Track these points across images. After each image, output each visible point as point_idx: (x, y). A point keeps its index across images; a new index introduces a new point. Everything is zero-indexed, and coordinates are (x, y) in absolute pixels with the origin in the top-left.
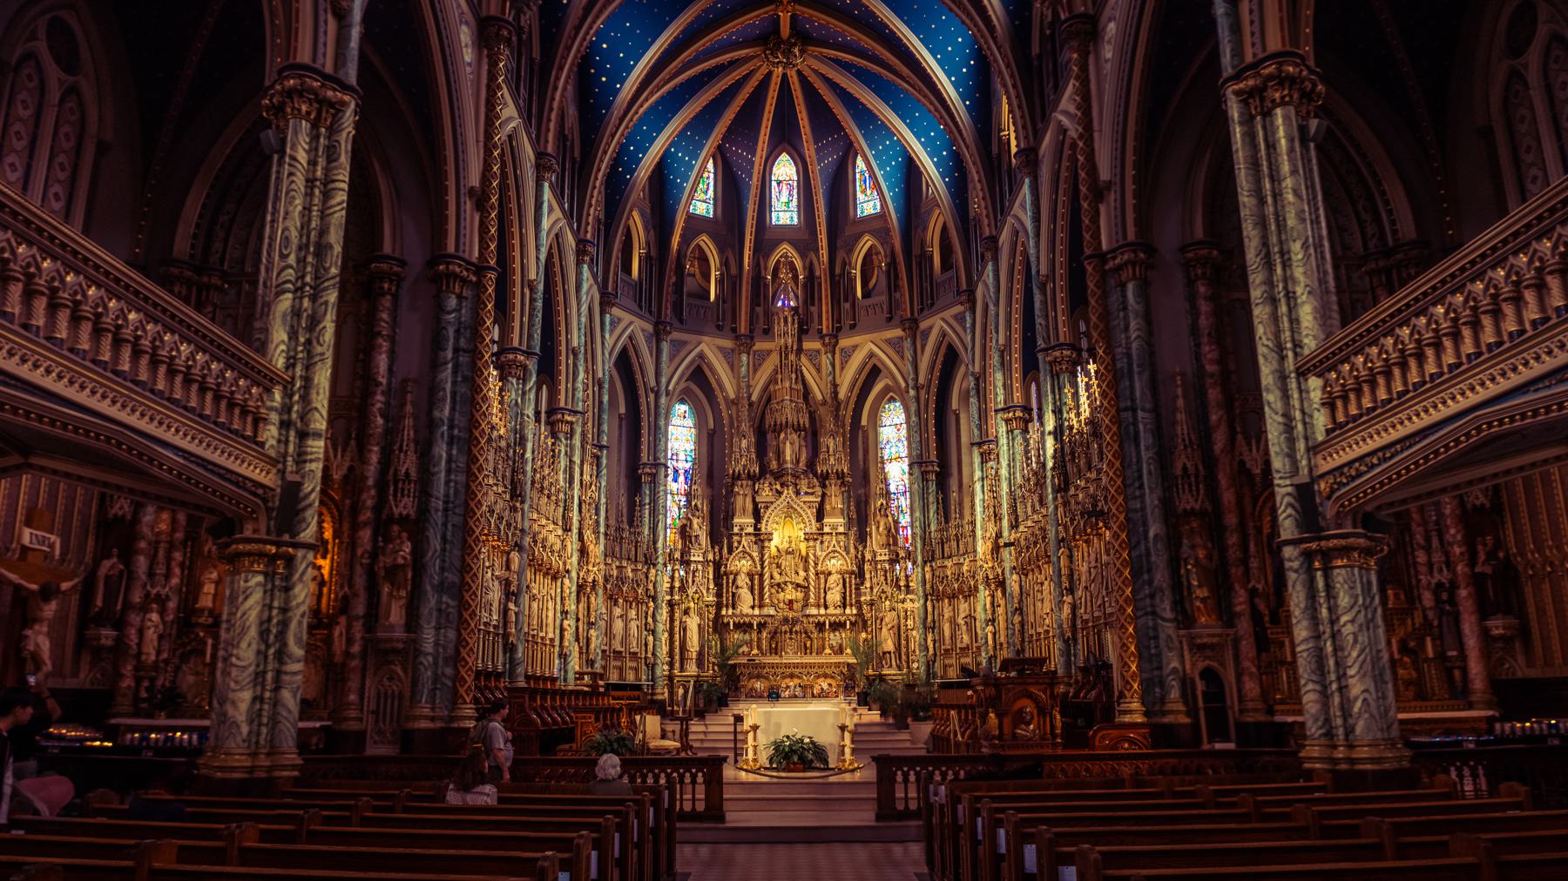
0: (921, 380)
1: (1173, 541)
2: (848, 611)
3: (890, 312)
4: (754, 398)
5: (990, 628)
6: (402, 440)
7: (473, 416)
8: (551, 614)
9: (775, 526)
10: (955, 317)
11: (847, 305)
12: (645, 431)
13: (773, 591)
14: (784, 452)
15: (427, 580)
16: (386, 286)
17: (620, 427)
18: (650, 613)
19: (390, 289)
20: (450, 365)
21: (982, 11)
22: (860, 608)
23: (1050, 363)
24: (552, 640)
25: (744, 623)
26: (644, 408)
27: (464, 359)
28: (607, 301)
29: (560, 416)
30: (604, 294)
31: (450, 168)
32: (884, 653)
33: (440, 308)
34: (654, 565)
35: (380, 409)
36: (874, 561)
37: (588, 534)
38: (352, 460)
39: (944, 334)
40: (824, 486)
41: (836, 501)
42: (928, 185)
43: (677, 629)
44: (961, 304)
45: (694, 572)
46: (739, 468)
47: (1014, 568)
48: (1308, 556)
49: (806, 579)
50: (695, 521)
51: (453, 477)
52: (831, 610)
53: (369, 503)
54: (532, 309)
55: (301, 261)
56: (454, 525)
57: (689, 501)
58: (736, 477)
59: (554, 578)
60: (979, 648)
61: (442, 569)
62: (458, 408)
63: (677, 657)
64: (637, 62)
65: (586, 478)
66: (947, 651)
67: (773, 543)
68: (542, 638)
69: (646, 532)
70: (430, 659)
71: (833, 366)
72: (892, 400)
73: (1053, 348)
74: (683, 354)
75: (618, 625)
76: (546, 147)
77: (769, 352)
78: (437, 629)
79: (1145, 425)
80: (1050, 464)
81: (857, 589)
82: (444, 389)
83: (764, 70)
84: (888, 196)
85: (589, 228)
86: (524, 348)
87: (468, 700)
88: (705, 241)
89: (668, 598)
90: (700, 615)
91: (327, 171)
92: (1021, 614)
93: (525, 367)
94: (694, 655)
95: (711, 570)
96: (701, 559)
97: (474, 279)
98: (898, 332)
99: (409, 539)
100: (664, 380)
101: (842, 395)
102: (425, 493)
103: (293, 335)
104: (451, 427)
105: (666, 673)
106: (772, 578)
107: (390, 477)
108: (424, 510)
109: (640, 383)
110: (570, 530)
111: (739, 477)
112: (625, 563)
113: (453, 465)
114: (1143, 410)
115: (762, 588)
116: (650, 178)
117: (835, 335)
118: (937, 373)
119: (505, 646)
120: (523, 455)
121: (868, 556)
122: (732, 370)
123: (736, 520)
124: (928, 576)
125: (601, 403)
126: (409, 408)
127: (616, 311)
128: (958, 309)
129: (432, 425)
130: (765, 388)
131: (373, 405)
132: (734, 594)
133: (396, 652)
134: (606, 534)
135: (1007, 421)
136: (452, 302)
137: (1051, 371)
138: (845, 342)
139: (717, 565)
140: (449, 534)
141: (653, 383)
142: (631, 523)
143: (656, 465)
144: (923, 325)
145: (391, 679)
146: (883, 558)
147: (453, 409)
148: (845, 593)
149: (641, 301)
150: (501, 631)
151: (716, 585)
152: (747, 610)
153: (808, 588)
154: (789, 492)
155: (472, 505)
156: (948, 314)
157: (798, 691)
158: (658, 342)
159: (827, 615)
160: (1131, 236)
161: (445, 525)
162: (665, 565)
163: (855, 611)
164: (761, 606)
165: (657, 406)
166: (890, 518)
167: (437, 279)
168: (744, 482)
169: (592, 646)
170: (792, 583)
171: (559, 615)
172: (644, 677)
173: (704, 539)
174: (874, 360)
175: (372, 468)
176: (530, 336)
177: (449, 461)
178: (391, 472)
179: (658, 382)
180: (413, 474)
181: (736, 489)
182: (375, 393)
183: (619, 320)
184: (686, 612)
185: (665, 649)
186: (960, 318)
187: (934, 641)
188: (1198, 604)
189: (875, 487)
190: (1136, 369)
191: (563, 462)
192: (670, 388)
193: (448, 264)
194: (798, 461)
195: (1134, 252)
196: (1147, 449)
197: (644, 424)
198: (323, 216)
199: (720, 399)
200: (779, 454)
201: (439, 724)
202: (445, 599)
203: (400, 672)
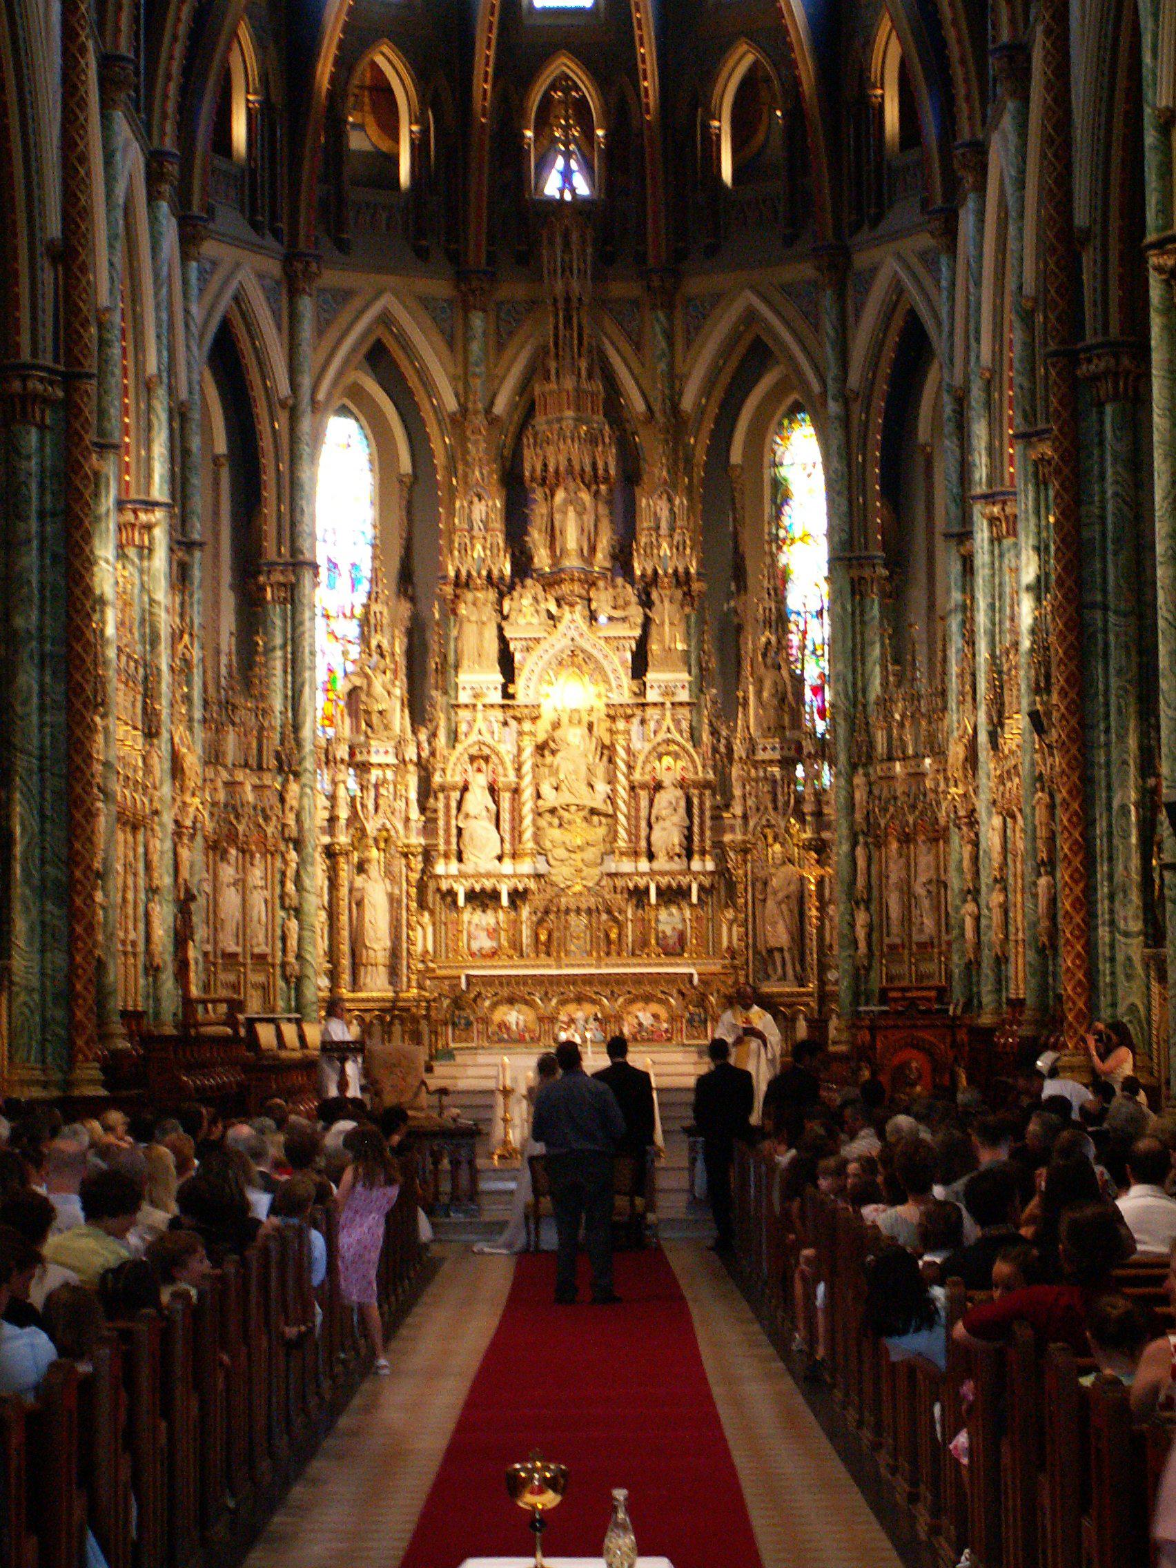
0: (854, 380)
2: (696, 865)
4: (500, 407)
5: (970, 907)
18: (290, 873)
20: (35, 544)
22: (721, 859)
24: (134, 944)
25: (483, 890)
26: (266, 443)
28: (189, 239)
31: (21, 217)
32: (770, 951)
34: (297, 775)
36: (750, 759)
40: (647, 603)
43: (344, 904)
45: (376, 786)
49: (611, 799)
51: (48, 718)
52: (661, 863)
57: (364, 639)
58: (462, 583)
60: (949, 943)
61: (43, 861)
63: (346, 962)
66: (893, 947)
71: (671, 344)
75: (230, 900)
76: (116, 44)
79: (1117, 636)
80: (1026, 644)
81: (716, 818)
82: (29, 582)
89: (326, 840)
90: (389, 873)
95: (412, 780)
96: (391, 759)
98: (805, 271)
100: (306, 381)
101: (687, 403)
104: (42, 641)
105: (326, 994)
109: (258, 393)
112: (240, 776)
113: (48, 700)
114: (1117, 613)
115: (517, 819)
118: (885, 370)
121: (739, 750)
122: (451, 345)
125: (186, 452)
128: (925, 241)
132: (460, 830)
135: (993, 521)
137: (1036, 474)
138: (696, 286)
139: (425, 770)
140: (48, 806)
141: (284, 389)
144: (861, 260)
147: (42, 611)
148: (690, 828)
151: (423, 809)
153: (613, 817)
154: (573, 618)
158: (293, 293)
159: (652, 873)
160: (1114, 330)
163: (710, 866)
165: (294, 439)
166: (784, 672)
168: (480, 595)
170: (580, 808)
171: (142, 896)
172: (281, 1004)
173: (399, 720)
177: (42, 693)
179: (294, 386)
183: (214, 264)
184: (361, 868)
185: (322, 945)
186: (929, 260)
187: (870, 928)
189: (758, 605)
190: (1110, 546)
192: (321, 396)
193: (24, 379)
194: (593, 549)
195: (1116, 357)
196: (1119, 673)
197: (269, 478)
201: (56, 1093)
202: (49, 906)
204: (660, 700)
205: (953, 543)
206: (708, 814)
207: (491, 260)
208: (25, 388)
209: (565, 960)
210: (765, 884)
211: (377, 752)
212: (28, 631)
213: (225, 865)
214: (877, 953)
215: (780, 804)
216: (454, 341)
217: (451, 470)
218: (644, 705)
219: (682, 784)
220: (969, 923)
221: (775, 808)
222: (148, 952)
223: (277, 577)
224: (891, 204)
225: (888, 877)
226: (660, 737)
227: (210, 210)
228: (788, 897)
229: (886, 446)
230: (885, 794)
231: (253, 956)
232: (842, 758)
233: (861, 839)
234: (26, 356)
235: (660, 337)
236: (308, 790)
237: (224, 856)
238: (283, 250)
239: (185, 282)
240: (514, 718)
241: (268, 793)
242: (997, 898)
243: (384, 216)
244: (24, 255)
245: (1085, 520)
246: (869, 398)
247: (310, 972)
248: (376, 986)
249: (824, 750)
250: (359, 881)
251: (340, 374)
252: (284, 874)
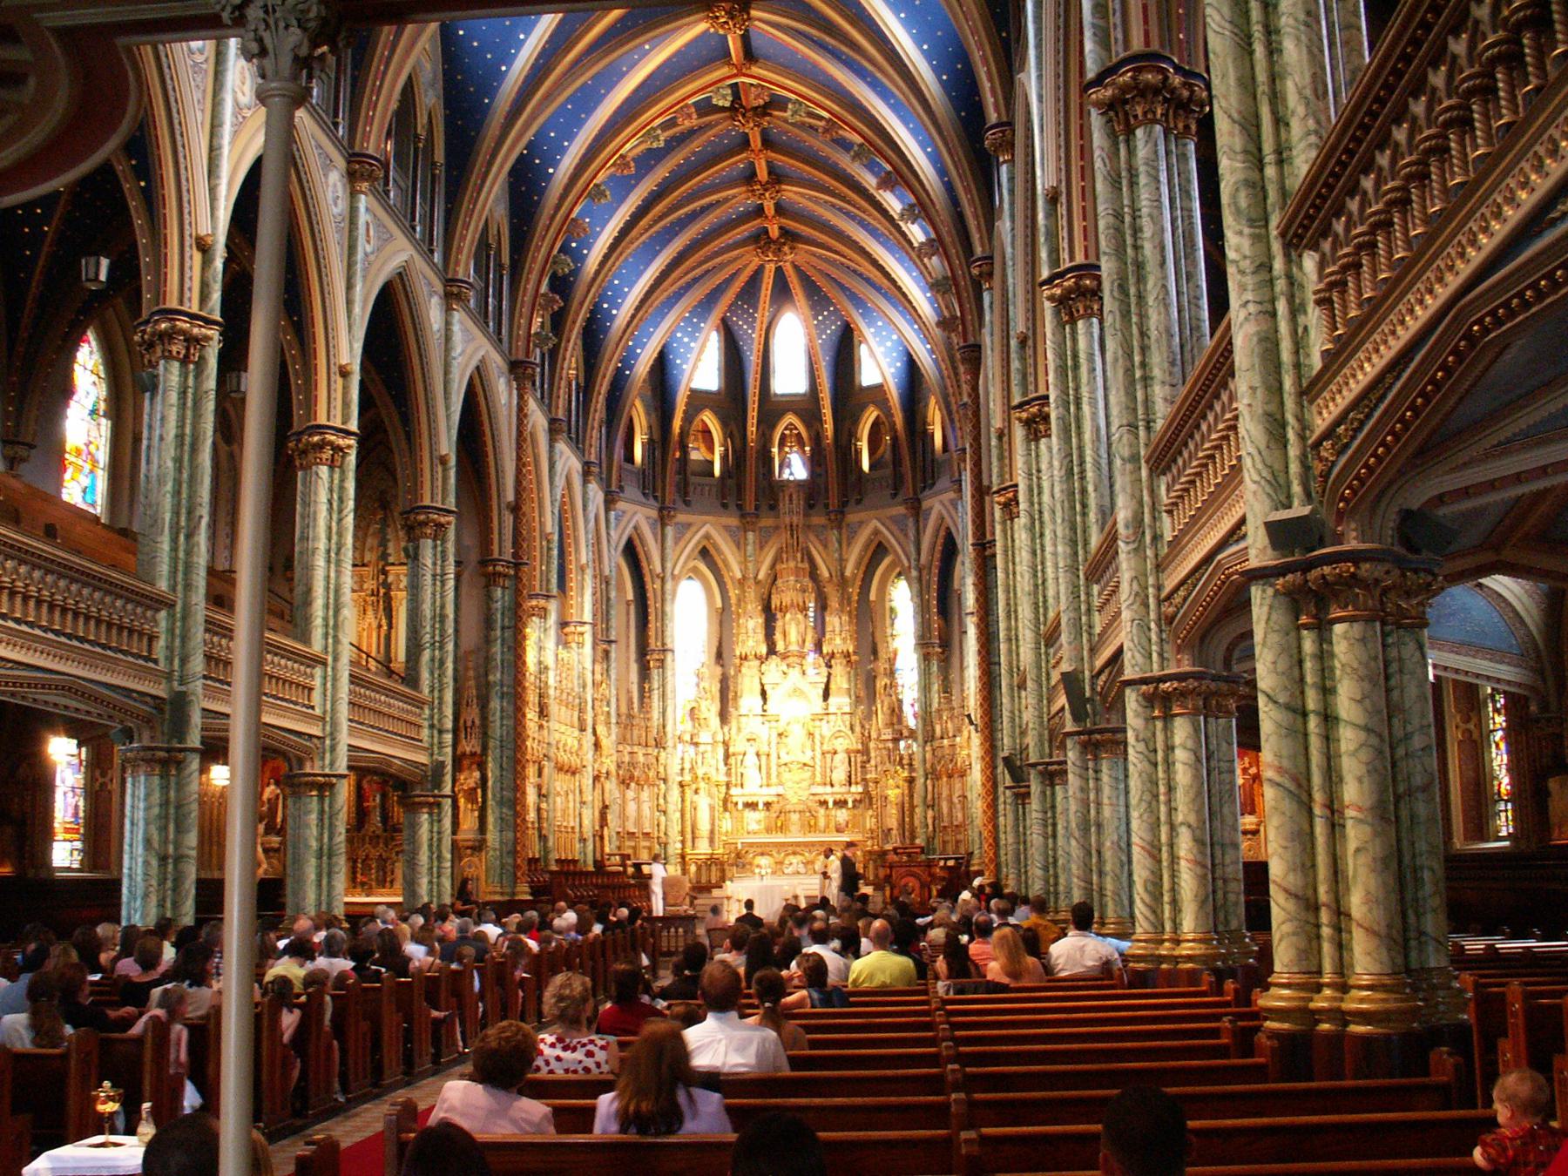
4: (761, 576)
17: (628, 614)
22: (866, 786)
26: (650, 594)
28: (609, 502)
33: (489, 597)
37: (601, 729)
40: (829, 666)
41: (841, 680)
48: (1017, 795)
52: (837, 789)
55: (433, 626)
58: (744, 658)
59: (574, 773)
64: (631, 287)
74: (688, 535)
75: (631, 808)
83: (756, 262)
88: (709, 419)
90: (710, 795)
91: (443, 567)
93: (545, 609)
95: (721, 751)
100: (669, 565)
101: (848, 573)
103: (432, 673)
108: (485, 748)
109: (646, 571)
116: (652, 367)
118: (937, 555)
121: (874, 735)
122: (738, 546)
124: (928, 756)
128: (952, 495)
136: (499, 592)
138: (852, 518)
139: (726, 744)
141: (658, 569)
144: (925, 504)
154: (795, 673)
157: (802, 869)
158: (663, 525)
165: (663, 593)
167: (487, 576)
173: (715, 721)
174: (880, 538)
177: (502, 710)
180: (477, 722)
184: (696, 792)
187: (934, 819)
192: (676, 572)
198: (442, 597)
199: (727, 579)
201: (507, 898)
207: (757, 508)
216: (739, 545)
217: (739, 605)
219: (848, 752)
223: (656, 656)
227: (621, 488)
234: (496, 555)
237: (628, 787)
238: (657, 505)
244: (495, 507)
248: (703, 848)
249: (912, 734)
250: (696, 798)
251: (685, 563)
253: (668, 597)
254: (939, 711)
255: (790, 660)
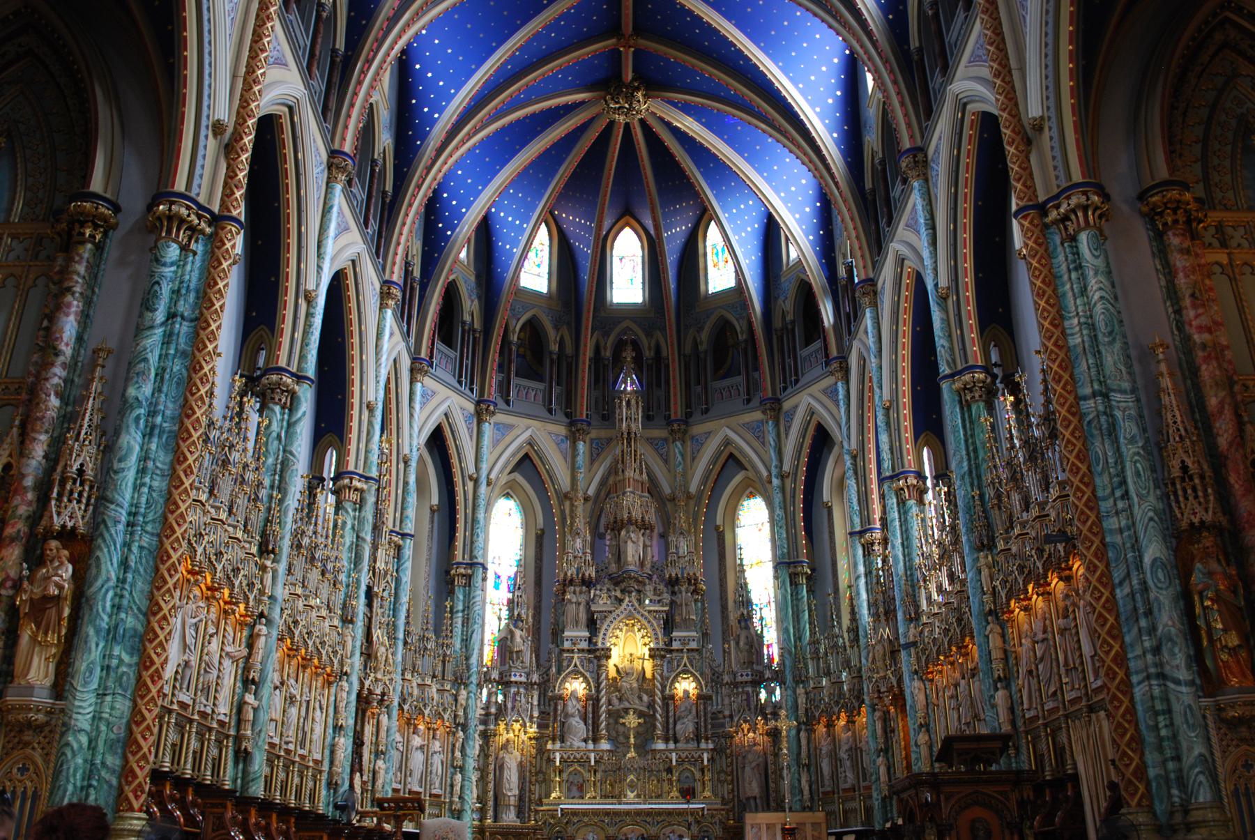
0: (786, 467)
1: (1181, 566)
2: (703, 745)
3: (748, 394)
4: (591, 492)
6: (81, 426)
7: (186, 400)
8: (319, 729)
9: (613, 640)
10: (825, 391)
11: (699, 389)
12: (460, 525)
13: (611, 721)
14: (626, 552)
15: (92, 622)
16: (88, 232)
17: (432, 522)
18: (458, 745)
19: (92, 236)
21: (857, 14)
23: (958, 392)
26: (460, 498)
27: (183, 328)
28: (416, 370)
29: (347, 481)
30: (415, 359)
32: (748, 799)
34: (466, 686)
35: (57, 385)
38: (10, 455)
39: (812, 413)
40: (673, 593)
42: (787, 239)
44: (832, 374)
46: (571, 572)
47: (916, 672)
49: (651, 705)
50: (518, 633)
51: (147, 480)
53: (23, 510)
54: (308, 325)
56: (141, 548)
57: (511, 610)
58: (567, 583)
60: (868, 788)
61: (117, 608)
62: (165, 389)
63: (491, 803)
65: (380, 565)
66: (825, 793)
67: (611, 663)
68: (303, 757)
69: (458, 646)
70: (84, 739)
72: (751, 495)
73: (960, 373)
74: (508, 439)
75: (417, 759)
76: (341, 145)
77: (609, 440)
78: (101, 695)
82: (146, 360)
84: (744, 263)
85: (396, 269)
86: (294, 369)
87: (136, 805)
89: (481, 728)
92: (928, 731)
93: (293, 395)
94: (513, 801)
96: (523, 679)
97: (208, 230)
98: (758, 415)
99: (70, 561)
100: (485, 467)
101: (693, 488)
102: (101, 498)
104: (152, 413)
106: (610, 703)
107: (57, 477)
108: (98, 523)
109: (456, 469)
110: (351, 622)
111: (571, 582)
113: (150, 464)
117: (687, 420)
119: (237, 752)
120: (281, 501)
123: (566, 634)
124: (802, 700)
125: (406, 483)
126: (95, 386)
127: (427, 380)
129: (125, 405)
130: (603, 482)
131: (47, 379)
132: (563, 724)
133: (38, 728)
134: (405, 643)
136: (173, 252)
137: (960, 402)
138: (697, 430)
142: (437, 632)
143: (472, 565)
144: (787, 405)
145: (24, 770)
146: (745, 678)
147: (158, 390)
149: (460, 376)
150: (232, 732)
152: (578, 744)
153: (654, 716)
155: (171, 518)
156: (816, 389)
158: (480, 422)
160: (1077, 177)
161: (127, 545)
162: (480, 686)
163: (711, 746)
164: (595, 740)
168: (578, 589)
169: (379, 782)
173: (528, 657)
174: (730, 449)
175: (34, 463)
176: (302, 358)
177: (145, 457)
178: (59, 469)
179: (477, 468)
181: (568, 596)
182: (53, 364)
186: (831, 393)
188: (1225, 657)
191: (349, 538)
192: (493, 476)
193: (172, 203)
195: (1085, 193)
197: (460, 516)
200: (619, 556)
203: (39, 761)
204: (681, 647)
205: (856, 538)
206: (709, 715)
208: (170, 210)
209: (624, 800)
210: (744, 757)
211: (515, 675)
212: (137, 399)
213: (416, 736)
214: (816, 798)
215: (752, 707)
218: (671, 651)
220: (883, 770)
221: (749, 710)
222: (330, 774)
224: (803, 375)
225: (821, 750)
226: (680, 669)
228: (758, 765)
229: (805, 501)
230: (818, 698)
231: (431, 795)
232: (789, 678)
233: (803, 727)
235: (678, 455)
236: (472, 695)
239: (412, 393)
240: (595, 657)
241: (446, 694)
242: (923, 738)
243: (533, 394)
245: (1068, 331)
246: (796, 474)
247: (467, 807)
252: (454, 746)
253: (482, 502)
254: (814, 643)
255: (623, 585)
